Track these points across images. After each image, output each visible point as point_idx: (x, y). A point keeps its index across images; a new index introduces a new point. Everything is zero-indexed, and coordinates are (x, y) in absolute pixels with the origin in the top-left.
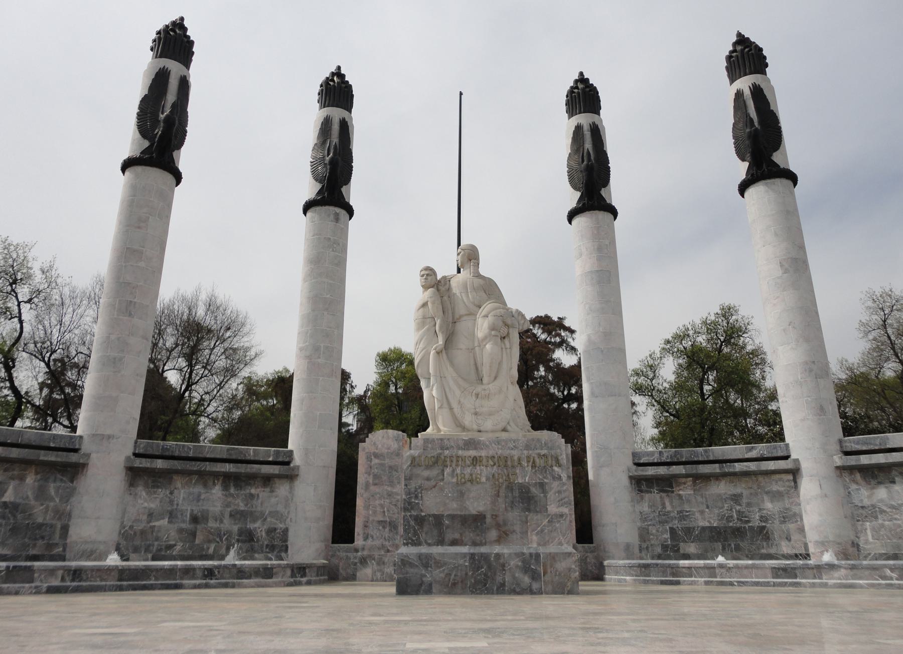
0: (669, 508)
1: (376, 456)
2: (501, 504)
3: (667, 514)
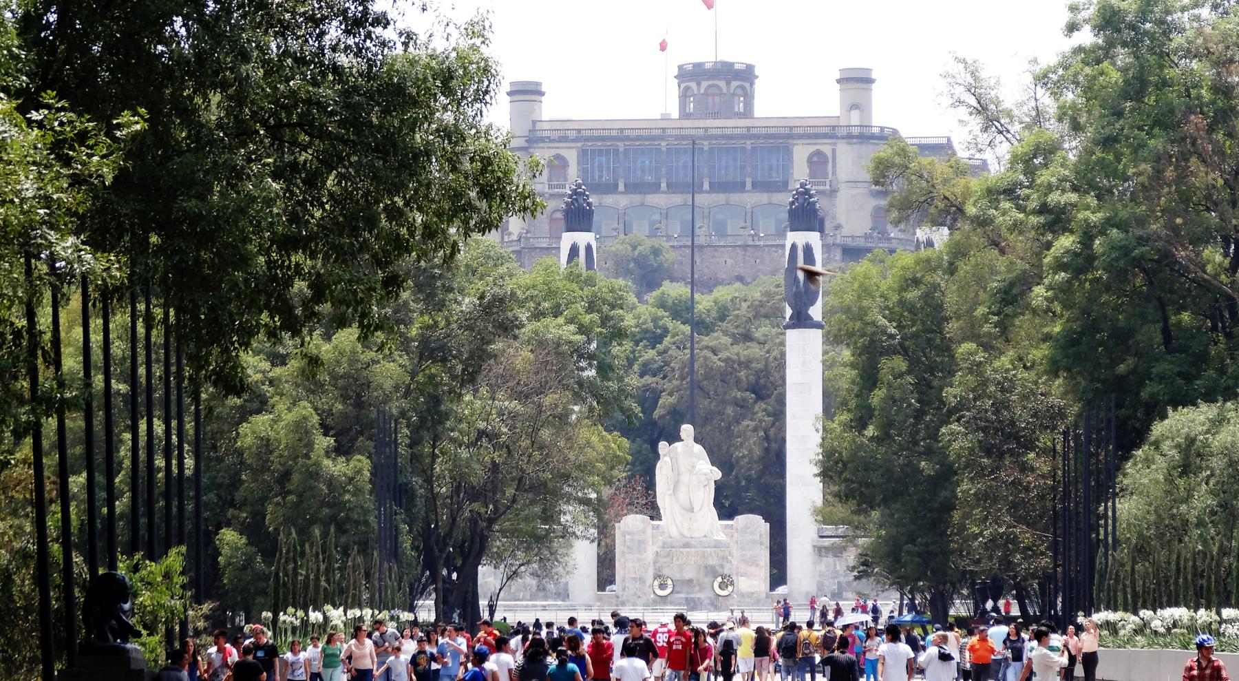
0: (838, 568)
1: (629, 533)
2: (701, 574)
3: (836, 572)
